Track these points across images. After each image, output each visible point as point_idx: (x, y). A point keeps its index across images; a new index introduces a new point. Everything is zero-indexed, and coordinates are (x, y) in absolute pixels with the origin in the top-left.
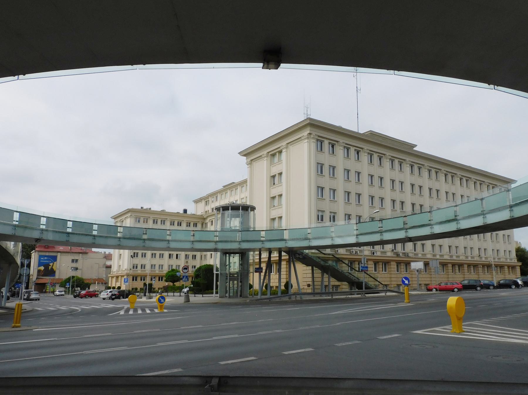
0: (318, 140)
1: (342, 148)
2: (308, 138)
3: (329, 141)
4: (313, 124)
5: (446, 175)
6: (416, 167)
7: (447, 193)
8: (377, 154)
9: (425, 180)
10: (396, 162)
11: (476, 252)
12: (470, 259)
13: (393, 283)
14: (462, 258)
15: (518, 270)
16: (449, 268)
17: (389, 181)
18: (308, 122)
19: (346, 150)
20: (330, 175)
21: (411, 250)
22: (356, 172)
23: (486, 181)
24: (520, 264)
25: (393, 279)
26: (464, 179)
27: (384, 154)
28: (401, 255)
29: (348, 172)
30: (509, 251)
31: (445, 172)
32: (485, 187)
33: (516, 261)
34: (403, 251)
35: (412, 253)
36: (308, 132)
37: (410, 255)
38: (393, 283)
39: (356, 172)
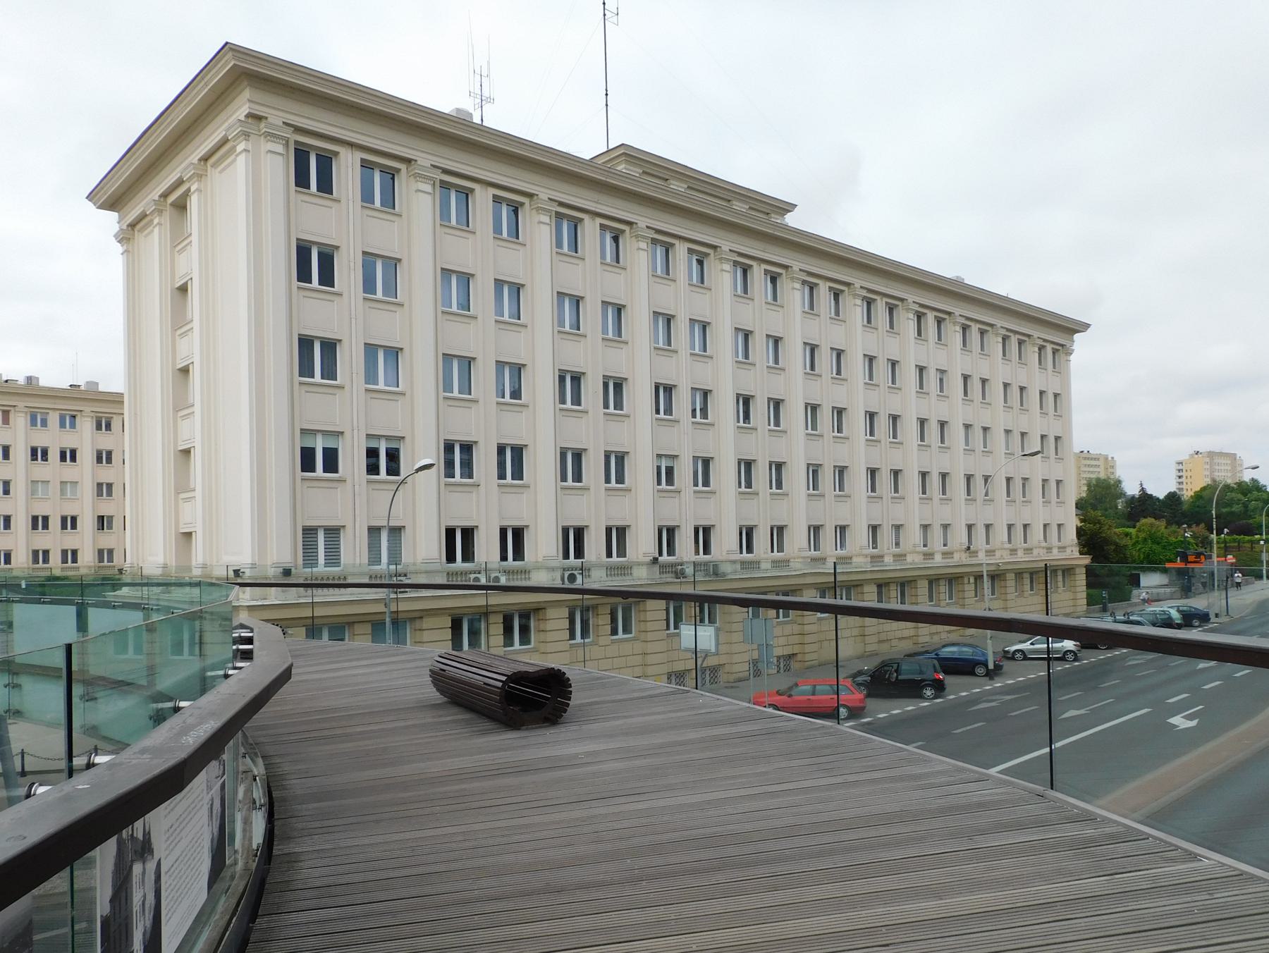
0: (559, 216)
1: (643, 245)
2: (247, 135)
3: (359, 155)
4: (243, 76)
5: (920, 317)
6: (880, 307)
7: (921, 369)
8: (764, 266)
9: (853, 332)
10: (823, 289)
11: (959, 537)
12: (938, 559)
13: (736, 658)
14: (914, 560)
15: (1081, 579)
16: (920, 592)
17: (800, 347)
18: (229, 63)
19: (660, 251)
20: (605, 331)
21: (728, 552)
22: (605, 304)
23: (1036, 334)
24: (1086, 560)
25: (807, 639)
26: (975, 328)
27: (630, 223)
28: (689, 570)
29: (669, 321)
30: (1059, 526)
31: (864, 293)
32: (953, 334)
33: (1077, 554)
34: (702, 557)
35: (734, 562)
36: (242, 113)
37: (726, 568)
38: (736, 658)
39: (605, 304)
